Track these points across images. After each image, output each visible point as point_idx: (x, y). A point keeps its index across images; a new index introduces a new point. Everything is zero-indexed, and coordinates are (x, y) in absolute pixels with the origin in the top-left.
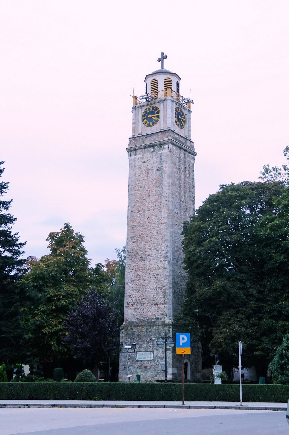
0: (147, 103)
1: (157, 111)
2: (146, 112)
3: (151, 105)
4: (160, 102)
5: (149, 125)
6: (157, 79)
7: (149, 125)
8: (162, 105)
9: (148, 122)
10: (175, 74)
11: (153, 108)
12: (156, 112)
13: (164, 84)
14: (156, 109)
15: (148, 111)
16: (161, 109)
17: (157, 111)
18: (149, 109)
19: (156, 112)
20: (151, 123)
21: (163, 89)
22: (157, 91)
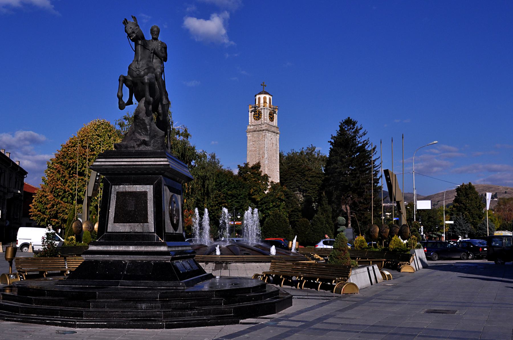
4: (261, 109)
5: (256, 120)
7: (257, 119)
9: (256, 118)
14: (260, 112)
16: (262, 112)
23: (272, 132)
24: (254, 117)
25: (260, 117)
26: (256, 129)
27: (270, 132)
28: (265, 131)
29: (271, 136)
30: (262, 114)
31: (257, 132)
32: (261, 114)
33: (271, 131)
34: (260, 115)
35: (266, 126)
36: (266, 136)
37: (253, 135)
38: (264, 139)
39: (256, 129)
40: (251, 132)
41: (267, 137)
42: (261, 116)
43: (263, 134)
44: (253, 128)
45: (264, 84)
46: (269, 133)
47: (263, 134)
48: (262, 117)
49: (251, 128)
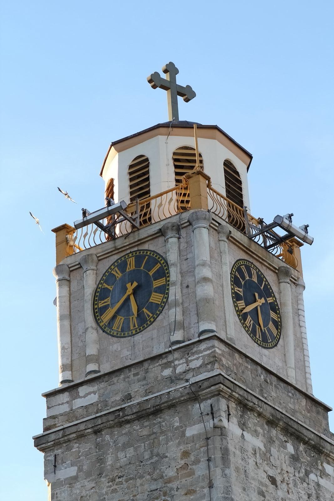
0: (111, 245)
1: (158, 266)
2: (108, 277)
3: (128, 251)
4: (161, 233)
6: (148, 155)
8: (173, 241)
10: (215, 128)
11: (139, 259)
12: (151, 273)
13: (173, 169)
15: (119, 275)
16: (172, 257)
17: (158, 266)
18: (122, 265)
19: (151, 273)
20: (134, 320)
21: (173, 184)
22: (150, 196)
23: (271, 423)
24: (98, 312)
25: (156, 298)
26: (129, 397)
27: (252, 420)
28: (205, 406)
29: (266, 456)
30: (174, 274)
31: (136, 426)
32: (163, 273)
33: (268, 412)
34: (157, 284)
35: (214, 360)
36: (217, 441)
37: (101, 460)
38: (200, 470)
39: (129, 397)
40: (81, 436)
41: (225, 452)
42: (164, 290)
43: (192, 431)
44: (93, 398)
45: (181, 81)
46: (243, 426)
47: (192, 431)
48: (175, 293)
49: (79, 403)
